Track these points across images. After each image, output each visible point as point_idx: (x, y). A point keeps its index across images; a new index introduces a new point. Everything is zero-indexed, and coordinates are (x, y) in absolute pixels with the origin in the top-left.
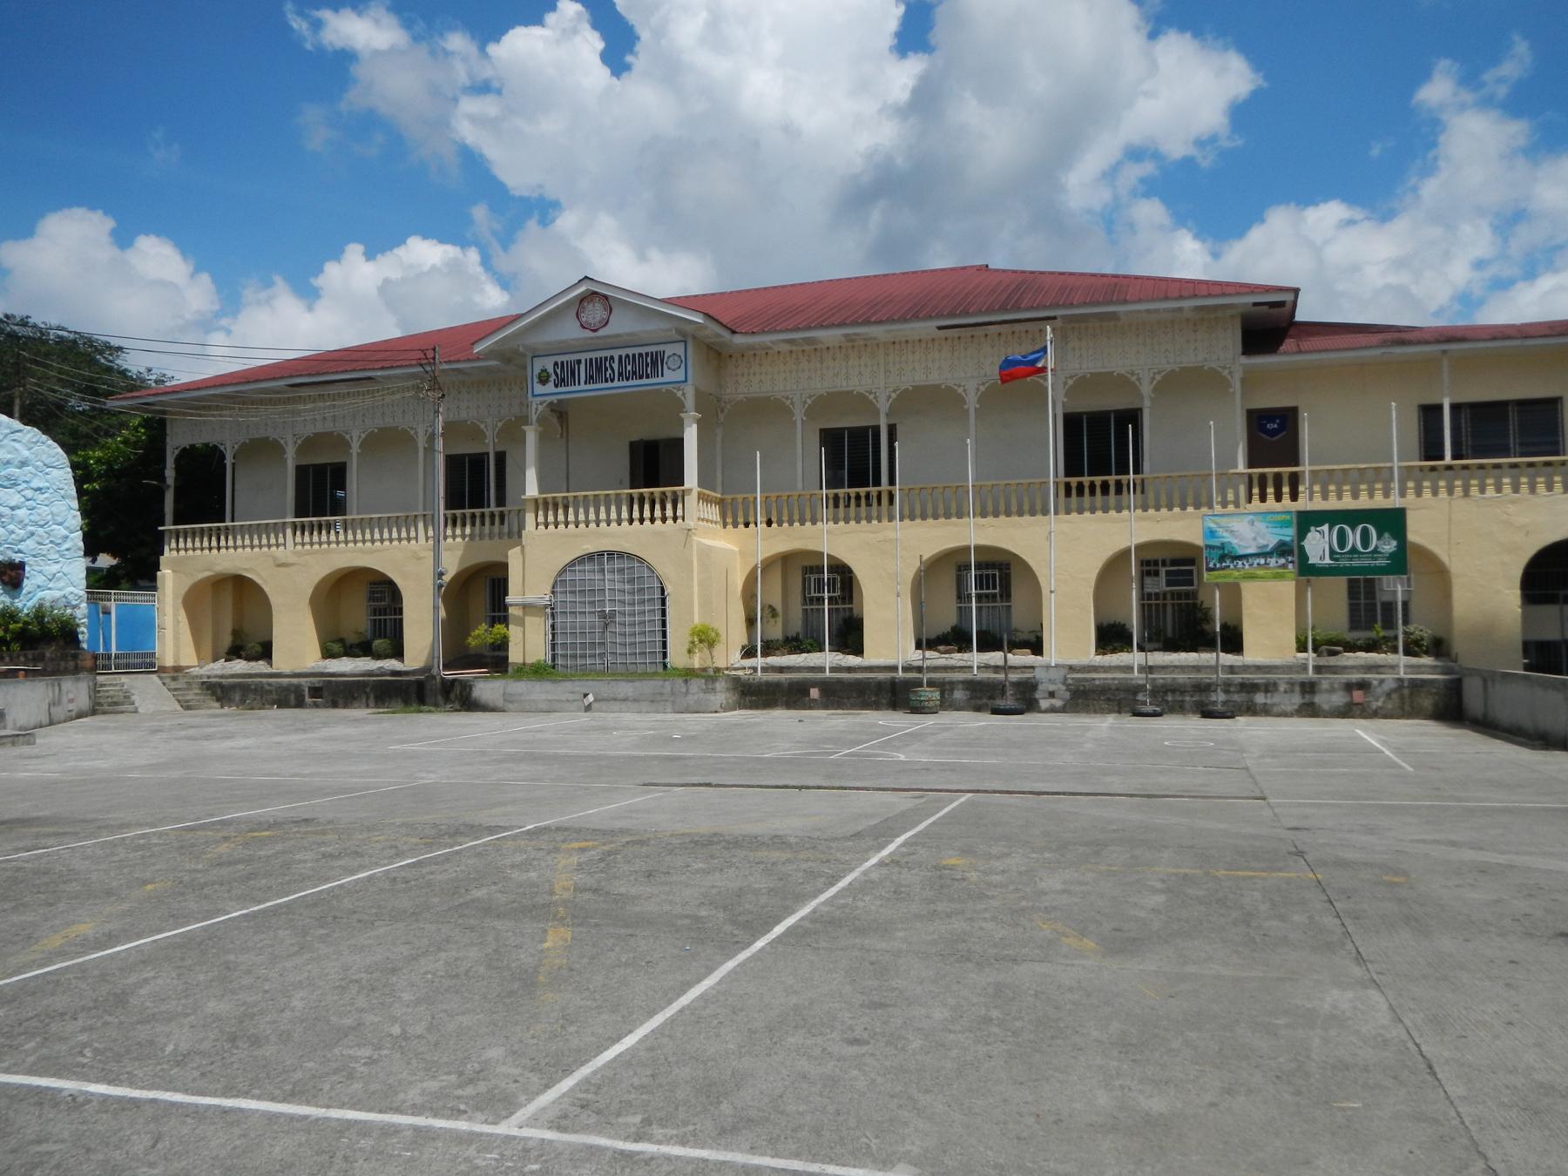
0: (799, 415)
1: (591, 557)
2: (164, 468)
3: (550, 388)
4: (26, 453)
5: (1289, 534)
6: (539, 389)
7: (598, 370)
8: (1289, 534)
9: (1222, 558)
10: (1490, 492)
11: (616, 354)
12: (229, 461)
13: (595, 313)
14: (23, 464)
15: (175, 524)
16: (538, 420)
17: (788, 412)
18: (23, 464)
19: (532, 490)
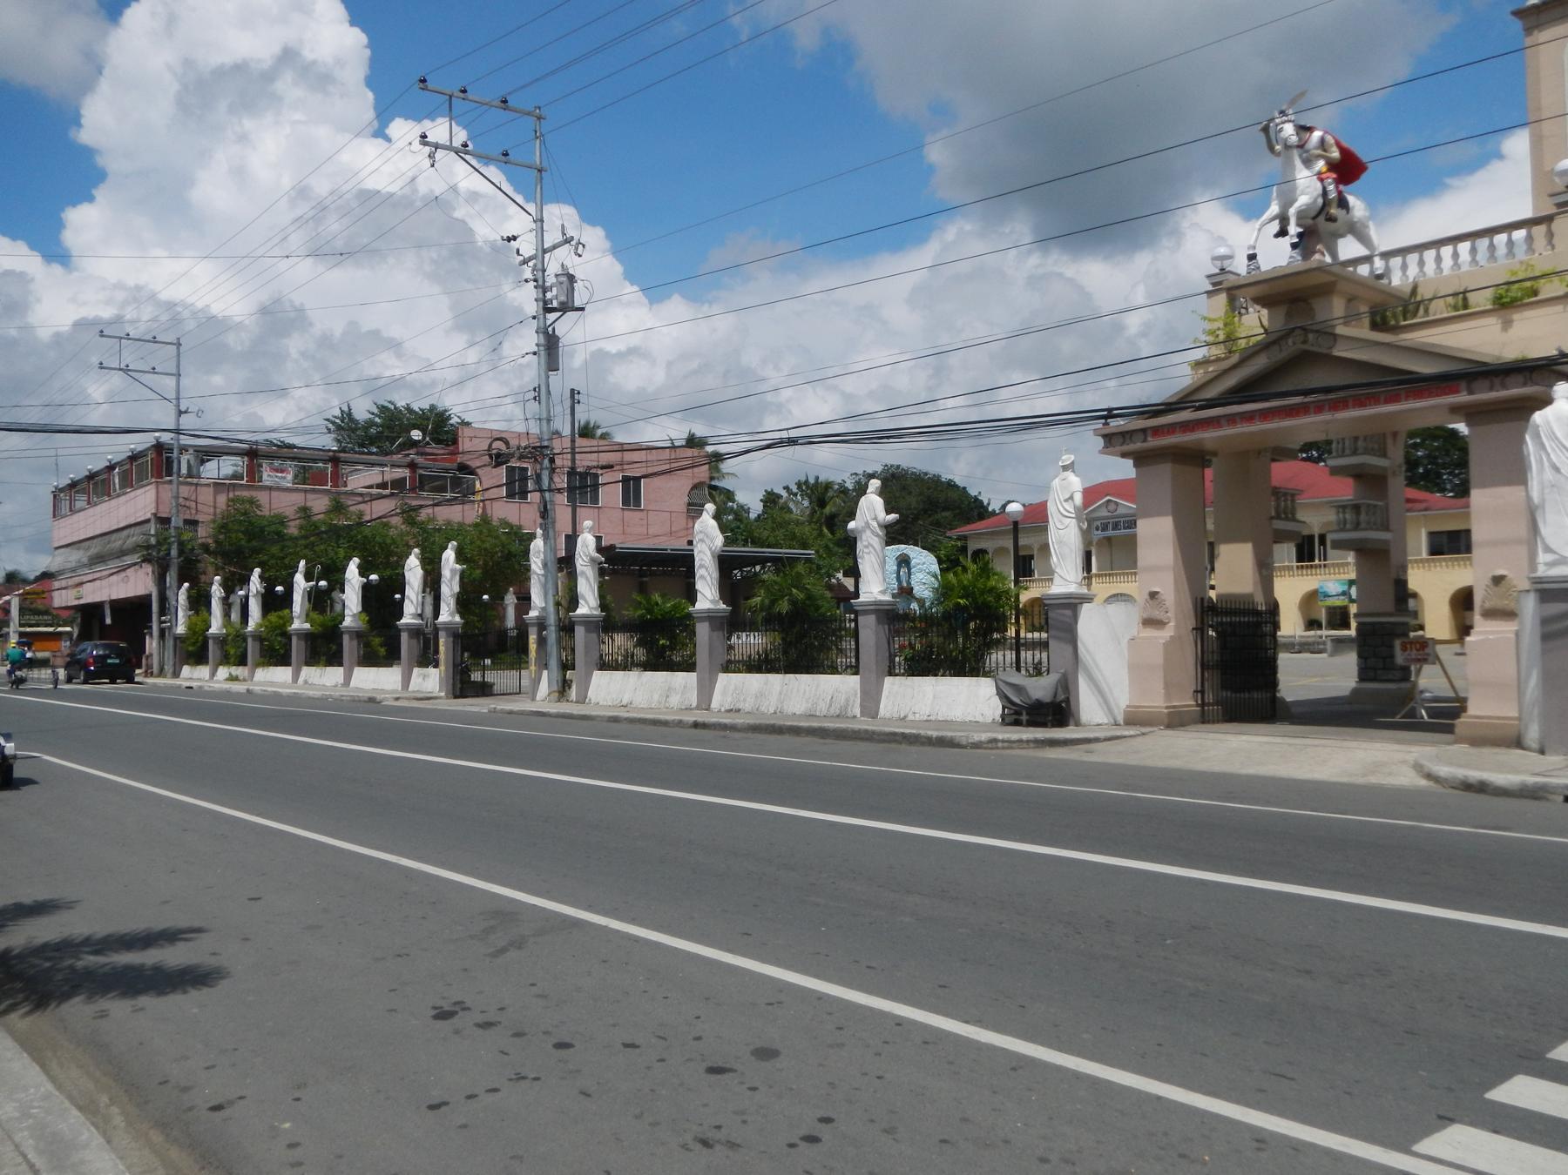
1: (1114, 596)
3: (1099, 532)
4: (924, 560)
5: (1345, 588)
6: (1096, 533)
7: (1116, 526)
8: (1345, 588)
9: (1325, 596)
10: (1438, 569)
11: (1122, 520)
13: (1112, 507)
14: (924, 563)
16: (1097, 544)
18: (924, 563)
19: (1094, 570)
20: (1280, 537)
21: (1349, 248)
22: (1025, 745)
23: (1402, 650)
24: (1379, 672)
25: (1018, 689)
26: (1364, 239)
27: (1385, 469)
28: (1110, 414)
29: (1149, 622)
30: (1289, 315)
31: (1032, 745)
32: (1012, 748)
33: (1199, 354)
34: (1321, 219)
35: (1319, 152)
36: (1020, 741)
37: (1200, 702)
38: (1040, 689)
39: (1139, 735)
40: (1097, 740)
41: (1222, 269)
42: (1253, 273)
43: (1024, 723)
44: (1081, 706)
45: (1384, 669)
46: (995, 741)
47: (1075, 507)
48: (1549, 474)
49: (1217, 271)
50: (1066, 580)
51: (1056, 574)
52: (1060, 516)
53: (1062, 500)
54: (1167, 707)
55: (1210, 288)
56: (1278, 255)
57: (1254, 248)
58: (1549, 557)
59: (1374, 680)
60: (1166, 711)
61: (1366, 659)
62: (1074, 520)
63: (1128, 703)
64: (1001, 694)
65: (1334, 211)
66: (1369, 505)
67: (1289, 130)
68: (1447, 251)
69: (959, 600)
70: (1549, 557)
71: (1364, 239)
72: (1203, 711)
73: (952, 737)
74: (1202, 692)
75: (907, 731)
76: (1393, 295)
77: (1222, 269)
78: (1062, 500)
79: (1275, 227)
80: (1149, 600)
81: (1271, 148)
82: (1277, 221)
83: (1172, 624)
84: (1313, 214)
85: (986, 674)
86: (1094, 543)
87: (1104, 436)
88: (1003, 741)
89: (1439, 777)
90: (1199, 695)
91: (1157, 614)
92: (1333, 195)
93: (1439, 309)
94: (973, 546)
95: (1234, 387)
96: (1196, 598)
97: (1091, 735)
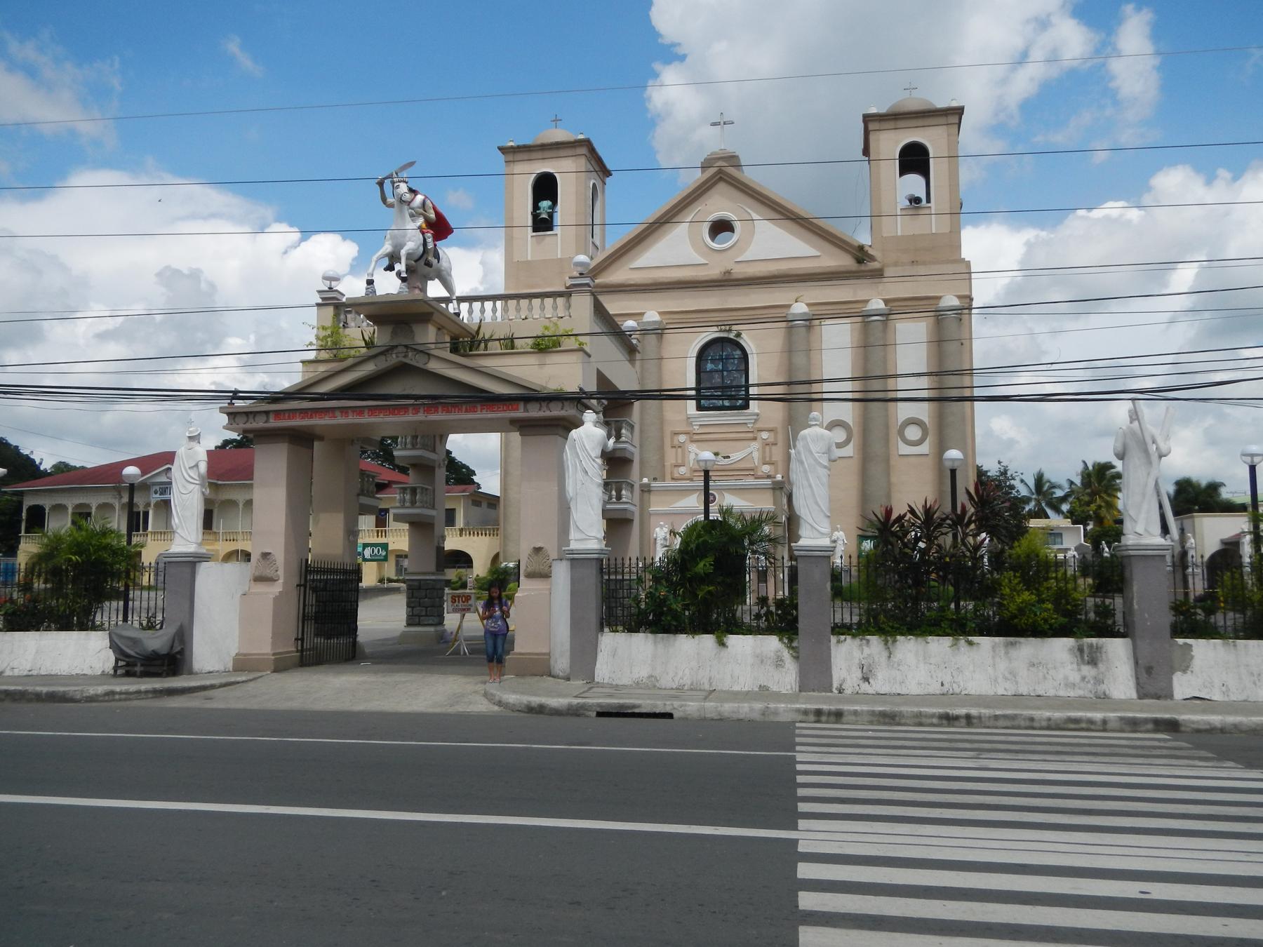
0: (241, 506)
2: (22, 512)
3: (158, 496)
6: (155, 496)
12: (47, 512)
15: (26, 533)
17: (238, 505)
19: (150, 529)
20: (365, 510)
21: (435, 289)
22: (143, 696)
23: (452, 602)
24: (422, 618)
25: (135, 642)
26: (447, 285)
27: (434, 461)
28: (236, 395)
29: (259, 579)
30: (394, 334)
31: (150, 696)
32: (130, 699)
33: (312, 355)
34: (422, 262)
35: (421, 211)
36: (139, 692)
37: (299, 648)
38: (156, 642)
39: (251, 680)
40: (212, 687)
41: (330, 288)
42: (371, 295)
43: (138, 674)
44: (194, 656)
45: (426, 615)
46: (113, 693)
47: (199, 474)
48: (580, 475)
49: (327, 289)
50: (189, 541)
51: (176, 535)
52: (184, 480)
53: (187, 468)
54: (274, 654)
55: (320, 301)
56: (389, 285)
57: (372, 275)
58: (579, 536)
59: (419, 624)
60: (273, 657)
61: (413, 608)
62: (197, 486)
63: (237, 651)
64: (113, 646)
65: (431, 258)
66: (422, 488)
67: (403, 188)
68: (477, 305)
69: (71, 556)
70: (579, 536)
71: (447, 285)
72: (302, 656)
73: (64, 691)
74: (302, 640)
75: (12, 688)
76: (464, 329)
77: (330, 288)
78: (187, 468)
79: (386, 262)
80: (261, 560)
81: (384, 200)
82: (387, 259)
83: (281, 581)
84: (416, 258)
85: (94, 628)
86: (152, 505)
87: (229, 414)
88: (121, 693)
89: (509, 703)
90: (300, 642)
91: (268, 572)
92: (430, 246)
93: (495, 347)
94: (28, 502)
95: (345, 386)
96: (302, 560)
97: (208, 683)
